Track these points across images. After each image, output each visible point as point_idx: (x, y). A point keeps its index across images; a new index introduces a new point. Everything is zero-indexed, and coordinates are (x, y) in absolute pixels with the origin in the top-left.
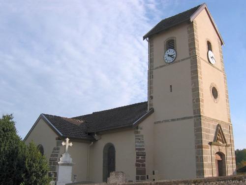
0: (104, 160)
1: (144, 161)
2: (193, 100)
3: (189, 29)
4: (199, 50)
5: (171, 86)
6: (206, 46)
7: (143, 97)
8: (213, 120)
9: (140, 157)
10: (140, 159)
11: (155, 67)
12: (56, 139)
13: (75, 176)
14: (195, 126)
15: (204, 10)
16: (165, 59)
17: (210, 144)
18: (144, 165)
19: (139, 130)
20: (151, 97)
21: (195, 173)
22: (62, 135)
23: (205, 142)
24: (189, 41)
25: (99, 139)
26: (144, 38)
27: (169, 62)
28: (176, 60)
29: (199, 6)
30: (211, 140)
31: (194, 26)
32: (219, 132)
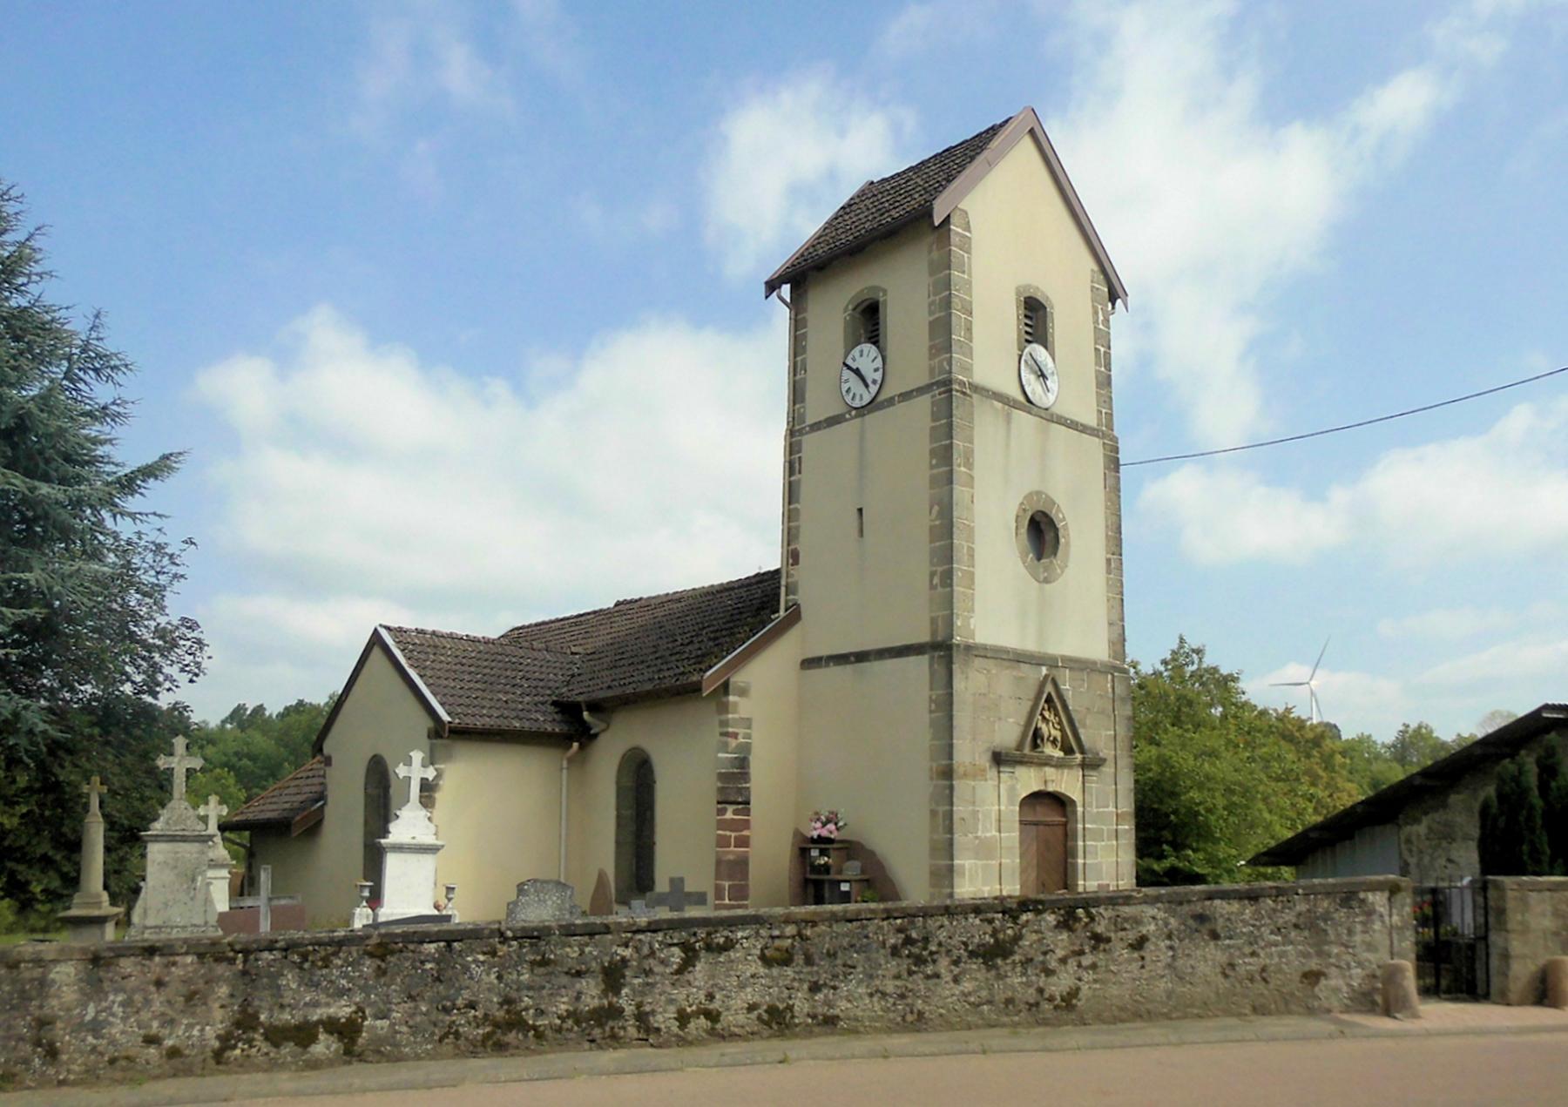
0: (619, 817)
1: (746, 825)
2: (932, 575)
3: (935, 255)
4: (970, 353)
5: (860, 510)
6: (1010, 320)
7: (771, 560)
8: (1019, 658)
9: (731, 808)
10: (729, 815)
11: (810, 420)
12: (429, 737)
13: (450, 889)
14: (931, 689)
15: (1027, 144)
16: (845, 387)
17: (999, 759)
18: (743, 842)
19: (732, 698)
20: (792, 556)
21: (926, 876)
22: (446, 718)
23: (969, 751)
24: (931, 313)
25: (603, 731)
26: (772, 286)
27: (857, 404)
28: (876, 402)
29: (993, 131)
30: (1008, 733)
31: (954, 239)
32: (1049, 700)
